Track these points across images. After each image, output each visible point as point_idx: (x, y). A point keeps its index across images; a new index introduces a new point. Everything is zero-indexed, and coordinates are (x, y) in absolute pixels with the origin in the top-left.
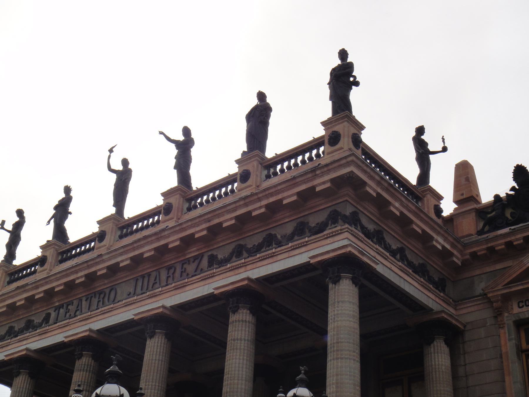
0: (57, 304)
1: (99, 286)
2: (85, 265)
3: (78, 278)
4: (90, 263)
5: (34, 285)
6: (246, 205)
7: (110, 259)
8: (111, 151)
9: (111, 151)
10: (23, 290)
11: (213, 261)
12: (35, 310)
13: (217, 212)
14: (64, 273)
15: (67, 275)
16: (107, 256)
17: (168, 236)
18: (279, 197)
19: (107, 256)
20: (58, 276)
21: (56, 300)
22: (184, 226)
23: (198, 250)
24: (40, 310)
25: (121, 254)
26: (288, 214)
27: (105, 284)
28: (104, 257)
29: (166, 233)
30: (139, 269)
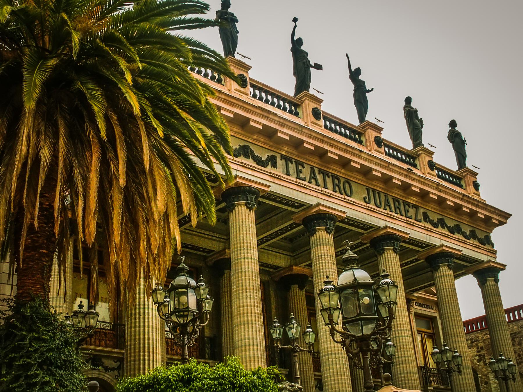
0: (284, 153)
1: (334, 170)
2: (345, 147)
3: (332, 152)
4: (348, 149)
5: (281, 121)
6: (462, 199)
7: (366, 160)
8: (295, 20)
9: (295, 20)
10: (266, 114)
11: (426, 217)
12: (256, 140)
13: (447, 191)
14: (321, 138)
15: (322, 141)
16: (366, 156)
17: (414, 180)
18: (478, 210)
19: (366, 156)
20: (314, 134)
21: (286, 149)
22: (426, 182)
23: (416, 201)
24: (261, 145)
25: (377, 164)
26: (468, 220)
27: (340, 172)
28: (363, 155)
29: (414, 177)
30: (374, 183)
